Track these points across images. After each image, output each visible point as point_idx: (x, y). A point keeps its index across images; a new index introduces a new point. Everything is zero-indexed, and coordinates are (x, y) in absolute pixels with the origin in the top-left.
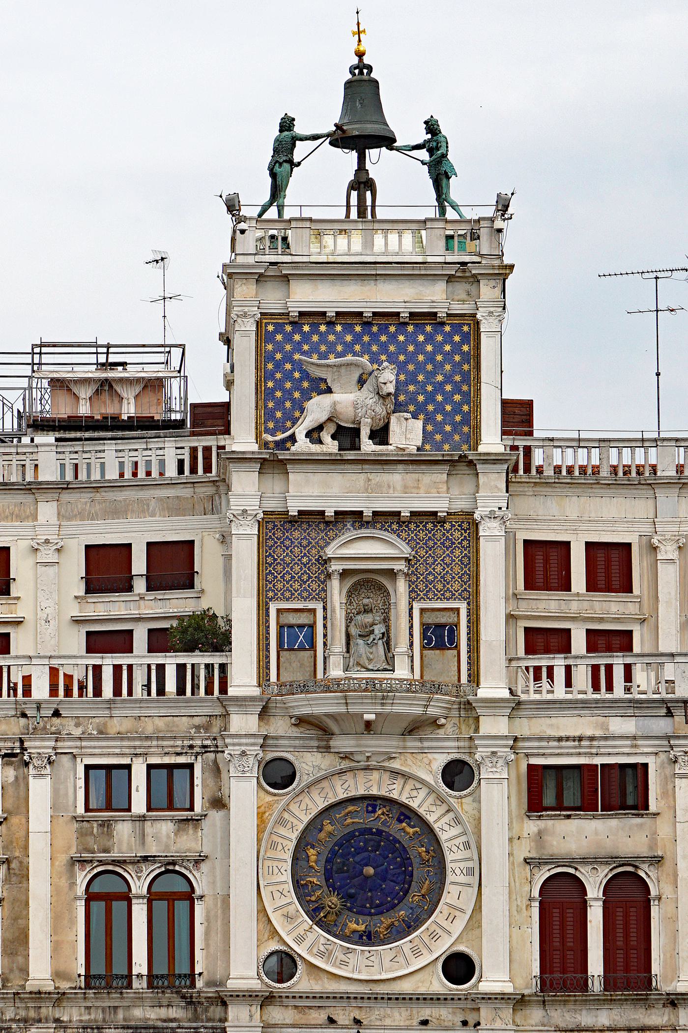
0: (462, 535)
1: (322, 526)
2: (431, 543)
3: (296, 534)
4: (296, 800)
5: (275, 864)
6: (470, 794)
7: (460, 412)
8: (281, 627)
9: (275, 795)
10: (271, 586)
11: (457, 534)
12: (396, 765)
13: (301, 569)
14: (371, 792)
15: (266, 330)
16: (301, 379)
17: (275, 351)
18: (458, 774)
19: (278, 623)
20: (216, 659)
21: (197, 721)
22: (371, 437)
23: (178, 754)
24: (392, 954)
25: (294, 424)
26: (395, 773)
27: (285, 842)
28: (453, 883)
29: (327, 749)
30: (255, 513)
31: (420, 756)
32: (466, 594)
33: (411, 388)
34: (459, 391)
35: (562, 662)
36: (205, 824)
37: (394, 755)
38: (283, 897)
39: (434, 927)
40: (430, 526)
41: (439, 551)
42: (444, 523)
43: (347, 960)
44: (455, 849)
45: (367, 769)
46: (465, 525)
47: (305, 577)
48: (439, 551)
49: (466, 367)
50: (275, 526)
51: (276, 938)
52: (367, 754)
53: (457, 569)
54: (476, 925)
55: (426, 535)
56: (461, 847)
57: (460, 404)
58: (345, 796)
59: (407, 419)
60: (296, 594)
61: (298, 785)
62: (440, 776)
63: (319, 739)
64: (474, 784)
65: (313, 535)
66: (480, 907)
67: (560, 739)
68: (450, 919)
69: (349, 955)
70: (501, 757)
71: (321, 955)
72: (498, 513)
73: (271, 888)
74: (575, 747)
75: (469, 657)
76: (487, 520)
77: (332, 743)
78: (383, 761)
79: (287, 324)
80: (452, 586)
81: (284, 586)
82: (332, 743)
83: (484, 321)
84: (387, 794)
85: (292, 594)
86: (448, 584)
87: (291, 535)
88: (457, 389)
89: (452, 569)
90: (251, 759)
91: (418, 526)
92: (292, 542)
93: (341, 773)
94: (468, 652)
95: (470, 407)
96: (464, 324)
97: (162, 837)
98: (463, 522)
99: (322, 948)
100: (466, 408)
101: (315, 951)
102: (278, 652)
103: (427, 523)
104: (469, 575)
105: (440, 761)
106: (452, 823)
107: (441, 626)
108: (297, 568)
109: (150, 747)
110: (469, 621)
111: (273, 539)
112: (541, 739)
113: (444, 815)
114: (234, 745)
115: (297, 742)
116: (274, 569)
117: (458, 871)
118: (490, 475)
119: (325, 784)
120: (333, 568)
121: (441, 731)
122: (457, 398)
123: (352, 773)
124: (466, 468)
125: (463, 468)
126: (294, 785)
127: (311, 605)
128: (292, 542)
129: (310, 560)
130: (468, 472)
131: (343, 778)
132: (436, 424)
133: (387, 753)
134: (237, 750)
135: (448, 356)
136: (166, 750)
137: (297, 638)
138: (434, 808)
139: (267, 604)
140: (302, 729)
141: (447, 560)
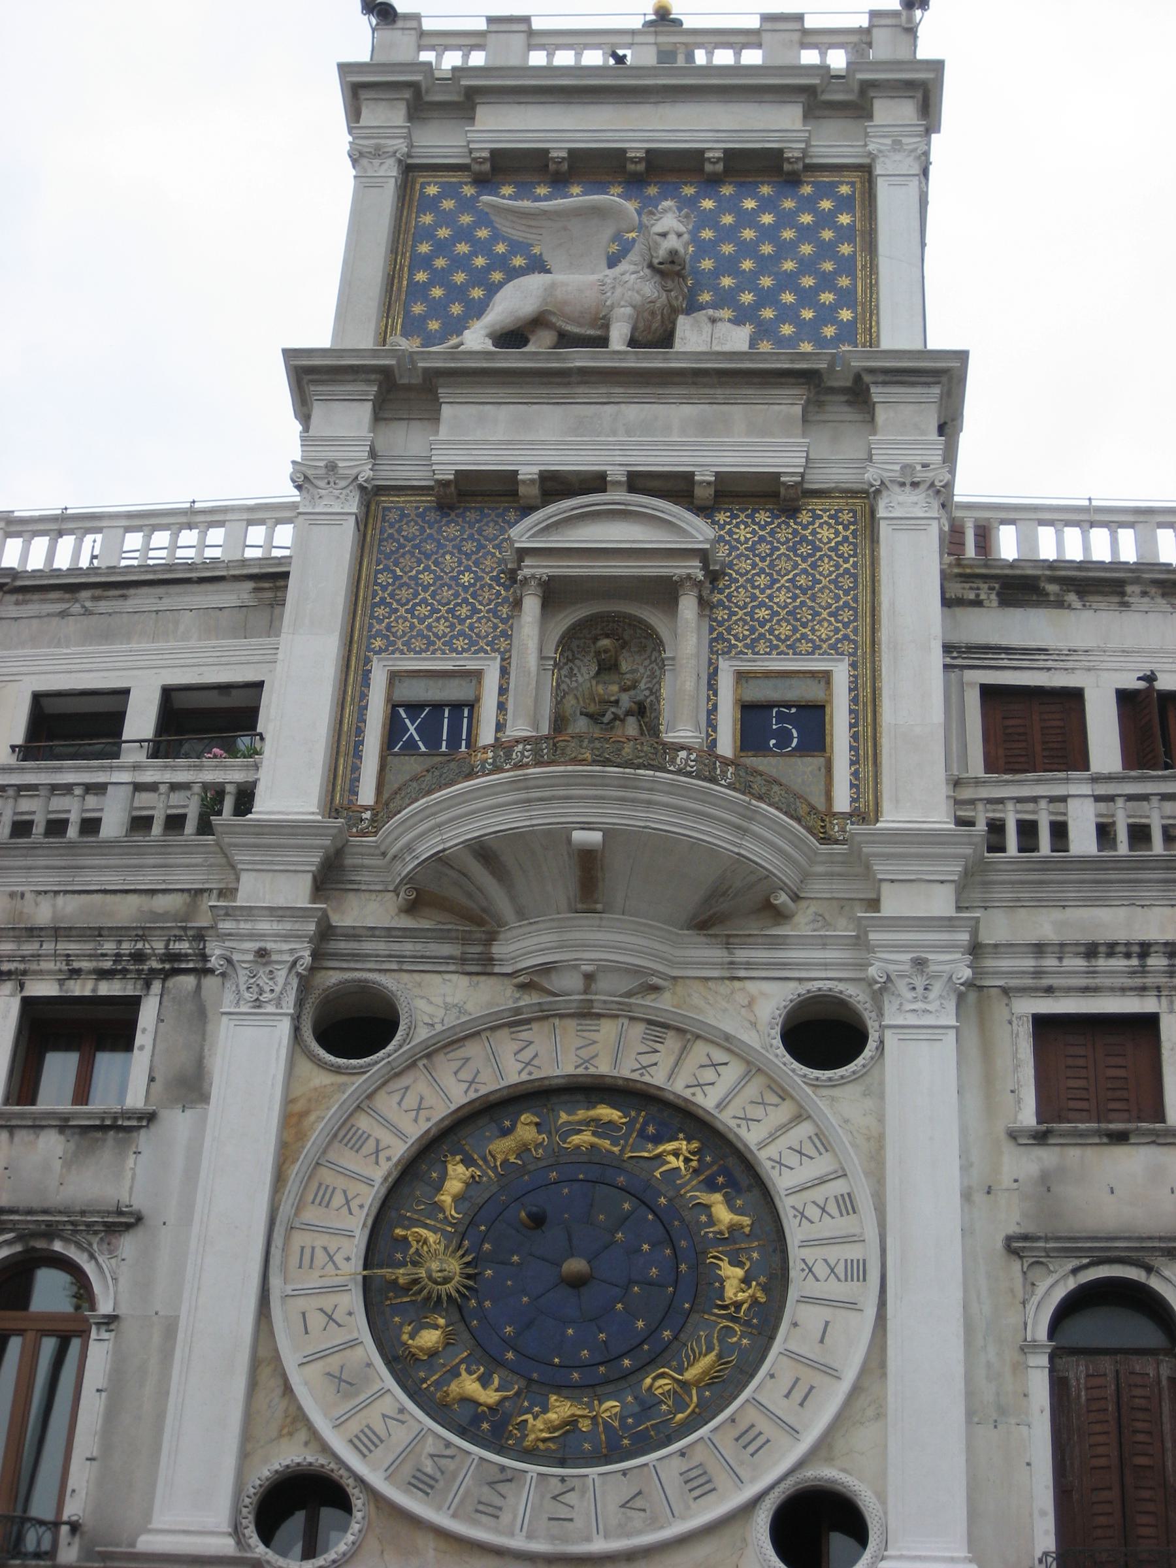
0: (837, 533)
2: (763, 548)
3: (452, 530)
4: (393, 1086)
5: (320, 1241)
6: (856, 1078)
7: (834, 321)
8: (393, 707)
9: (337, 1070)
11: (825, 533)
12: (665, 1003)
13: (456, 595)
14: (592, 1070)
15: (422, 194)
16: (488, 269)
17: (438, 224)
18: (826, 1036)
19: (389, 699)
20: (229, 773)
21: (162, 903)
23: (103, 974)
24: (626, 1489)
26: (659, 1026)
27: (355, 1188)
28: (805, 1300)
29: (482, 966)
30: (354, 472)
31: (725, 988)
32: (846, 647)
33: (727, 282)
36: (143, 1138)
37: (655, 980)
38: (330, 1321)
39: (753, 1415)
41: (782, 564)
43: (498, 1501)
44: (813, 1212)
45: (586, 1013)
46: (846, 517)
47: (464, 611)
48: (782, 564)
49: (845, 249)
50: (403, 516)
51: (302, 1435)
52: (588, 968)
54: (870, 1412)
55: (754, 532)
56: (832, 1208)
57: (834, 308)
58: (524, 1077)
62: (776, 1032)
63: (465, 940)
64: (871, 1044)
66: (883, 1365)
67: (1091, 951)
68: (797, 1395)
69: (501, 1487)
70: (937, 976)
71: (422, 1484)
73: (301, 1303)
74: (1132, 973)
75: (855, 774)
76: (896, 489)
77: (497, 950)
78: (629, 994)
79: (466, 184)
80: (813, 631)
81: (412, 627)
82: (497, 950)
83: (882, 159)
84: (635, 1076)
86: (804, 625)
88: (826, 282)
89: (813, 598)
90: (281, 975)
92: (440, 546)
93: (515, 1022)
94: (852, 763)
95: (855, 312)
96: (842, 183)
97: (31, 1169)
98: (841, 511)
99: (429, 1467)
100: (845, 315)
101: (407, 1470)
103: (757, 511)
106: (808, 1149)
108: (447, 593)
109: (37, 957)
110: (854, 700)
111: (398, 541)
112: (1039, 949)
113: (784, 1128)
114: (241, 937)
115: (408, 947)
116: (392, 596)
117: (821, 1270)
118: (902, 406)
119: (472, 1049)
120: (527, 572)
123: (546, 1026)
124: (846, 409)
125: (839, 410)
126: (390, 1048)
127: (472, 665)
128: (440, 546)
129: (478, 579)
130: (849, 417)
131: (525, 1035)
132: (780, 341)
133: (636, 971)
135: (806, 233)
136: (76, 965)
137: (431, 729)
138: (758, 1112)
139: (368, 661)
141: (802, 581)
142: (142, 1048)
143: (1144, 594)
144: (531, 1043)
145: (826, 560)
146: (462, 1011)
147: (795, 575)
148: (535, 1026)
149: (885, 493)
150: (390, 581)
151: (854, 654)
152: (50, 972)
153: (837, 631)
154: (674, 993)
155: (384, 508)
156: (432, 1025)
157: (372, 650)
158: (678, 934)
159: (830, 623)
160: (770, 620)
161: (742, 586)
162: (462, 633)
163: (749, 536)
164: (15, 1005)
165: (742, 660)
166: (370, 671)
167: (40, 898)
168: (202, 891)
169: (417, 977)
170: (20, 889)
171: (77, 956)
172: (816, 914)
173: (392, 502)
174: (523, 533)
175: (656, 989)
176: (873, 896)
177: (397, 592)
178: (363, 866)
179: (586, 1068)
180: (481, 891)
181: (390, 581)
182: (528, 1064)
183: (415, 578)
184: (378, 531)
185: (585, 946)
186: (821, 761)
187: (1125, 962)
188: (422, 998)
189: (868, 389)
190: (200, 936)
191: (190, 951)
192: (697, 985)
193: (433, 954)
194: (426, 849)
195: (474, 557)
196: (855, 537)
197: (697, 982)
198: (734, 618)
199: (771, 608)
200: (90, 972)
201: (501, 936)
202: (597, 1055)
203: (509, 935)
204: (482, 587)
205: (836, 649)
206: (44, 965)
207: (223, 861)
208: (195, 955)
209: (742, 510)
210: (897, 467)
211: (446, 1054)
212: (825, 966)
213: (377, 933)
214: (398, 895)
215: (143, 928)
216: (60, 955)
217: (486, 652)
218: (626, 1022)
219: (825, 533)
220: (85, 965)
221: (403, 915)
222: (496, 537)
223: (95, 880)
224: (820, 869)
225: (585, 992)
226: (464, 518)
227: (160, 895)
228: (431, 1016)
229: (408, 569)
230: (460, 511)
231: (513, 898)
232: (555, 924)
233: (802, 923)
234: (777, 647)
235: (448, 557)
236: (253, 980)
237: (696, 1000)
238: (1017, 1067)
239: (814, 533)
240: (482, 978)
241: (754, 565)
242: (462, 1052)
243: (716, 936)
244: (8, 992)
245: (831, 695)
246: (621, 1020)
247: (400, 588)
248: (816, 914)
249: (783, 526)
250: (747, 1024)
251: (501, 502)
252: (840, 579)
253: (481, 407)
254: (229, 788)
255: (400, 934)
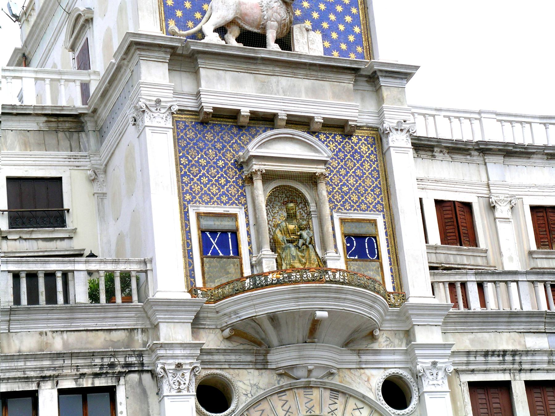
0: (369, 149)
1: (235, 130)
2: (341, 155)
3: (209, 136)
8: (203, 232)
10: (188, 188)
11: (364, 148)
22: (277, 41)
23: (96, 375)
25: (195, 25)
26: (336, 391)
29: (262, 365)
32: (379, 207)
34: (350, 14)
35: (473, 278)
40: (338, 138)
41: (350, 164)
42: (352, 136)
45: (308, 387)
46: (370, 140)
47: (223, 181)
48: (350, 164)
53: (368, 182)
55: (336, 146)
59: (307, 30)
60: (215, 199)
61: (237, 406)
65: (226, 138)
72: (404, 126)
78: (322, 378)
80: (366, 198)
81: (202, 189)
82: (270, 357)
85: (211, 198)
86: (362, 195)
87: (205, 137)
91: (327, 137)
92: (206, 145)
93: (281, 392)
95: (360, 28)
100: (357, 30)
102: (202, 260)
103: (335, 135)
104: (380, 188)
105: (377, 378)
107: (360, 238)
108: (214, 171)
115: (233, 358)
116: (189, 171)
118: (392, 89)
119: (265, 405)
121: (376, 346)
122: (348, 19)
124: (366, 84)
127: (232, 210)
128: (206, 145)
129: (226, 164)
131: (284, 398)
132: (332, 41)
133: (327, 367)
134: (171, 365)
139: (185, 207)
140: (235, 344)
141: (358, 172)
142: (121, 413)
143: (441, 152)
144: (287, 401)
145: (366, 162)
146: (258, 388)
147: (355, 170)
148: (287, 393)
149: (391, 134)
150: (187, 162)
151: (383, 211)
152: (70, 376)
153: (375, 199)
154: (339, 376)
155: (176, 121)
156: (247, 395)
157: (186, 201)
158: (341, 350)
159: (372, 195)
160: (349, 192)
161: (335, 174)
162: (224, 193)
163: (335, 148)
164: (55, 393)
165: (341, 213)
166: (188, 212)
167: (55, 334)
168: (134, 329)
169: (236, 371)
170: (44, 330)
171: (82, 366)
172: (387, 337)
173: (179, 118)
174: (254, 148)
175: (332, 374)
176: (407, 329)
177: (191, 169)
178: (207, 317)
179: (310, 412)
180: (264, 331)
181: (187, 162)
182: (287, 411)
183: (197, 162)
184: (176, 134)
185: (310, 358)
186: (378, 263)
187: (497, 359)
188: (240, 381)
189: (378, 78)
190: (140, 354)
191: (136, 362)
192: (347, 372)
193: (244, 360)
194: (245, 314)
195: (222, 152)
196: (376, 151)
197: (347, 370)
198: (335, 191)
199: (348, 186)
200: (90, 375)
201: (271, 352)
202: (313, 406)
203: (275, 351)
204: (228, 168)
205: (376, 208)
206: (66, 372)
207: (145, 315)
208: (139, 364)
209: (330, 134)
210: (396, 121)
211: (254, 408)
212: (394, 362)
213: (220, 351)
214: (222, 331)
215: (114, 351)
216: (73, 366)
217: (236, 205)
218: (323, 390)
219: (364, 148)
220: (85, 371)
221: (225, 340)
222: (229, 142)
223: (82, 325)
224: (388, 318)
225: (307, 378)
226: (214, 130)
227: (114, 332)
228: (246, 390)
229: (193, 156)
230: (211, 125)
231: (278, 335)
232: (297, 348)
233: (382, 343)
234: (353, 206)
235: (210, 151)
236: (175, 379)
237: (348, 379)
238: (465, 406)
239: (360, 148)
240: (263, 371)
241: (339, 163)
242: (260, 407)
243: (355, 350)
244: (50, 387)
245: (378, 231)
246: (321, 389)
247: (192, 167)
248: (387, 337)
249: (347, 144)
250: (368, 389)
251: (229, 122)
252: (373, 173)
253: (217, 71)
254: (133, 274)
255: (229, 351)
